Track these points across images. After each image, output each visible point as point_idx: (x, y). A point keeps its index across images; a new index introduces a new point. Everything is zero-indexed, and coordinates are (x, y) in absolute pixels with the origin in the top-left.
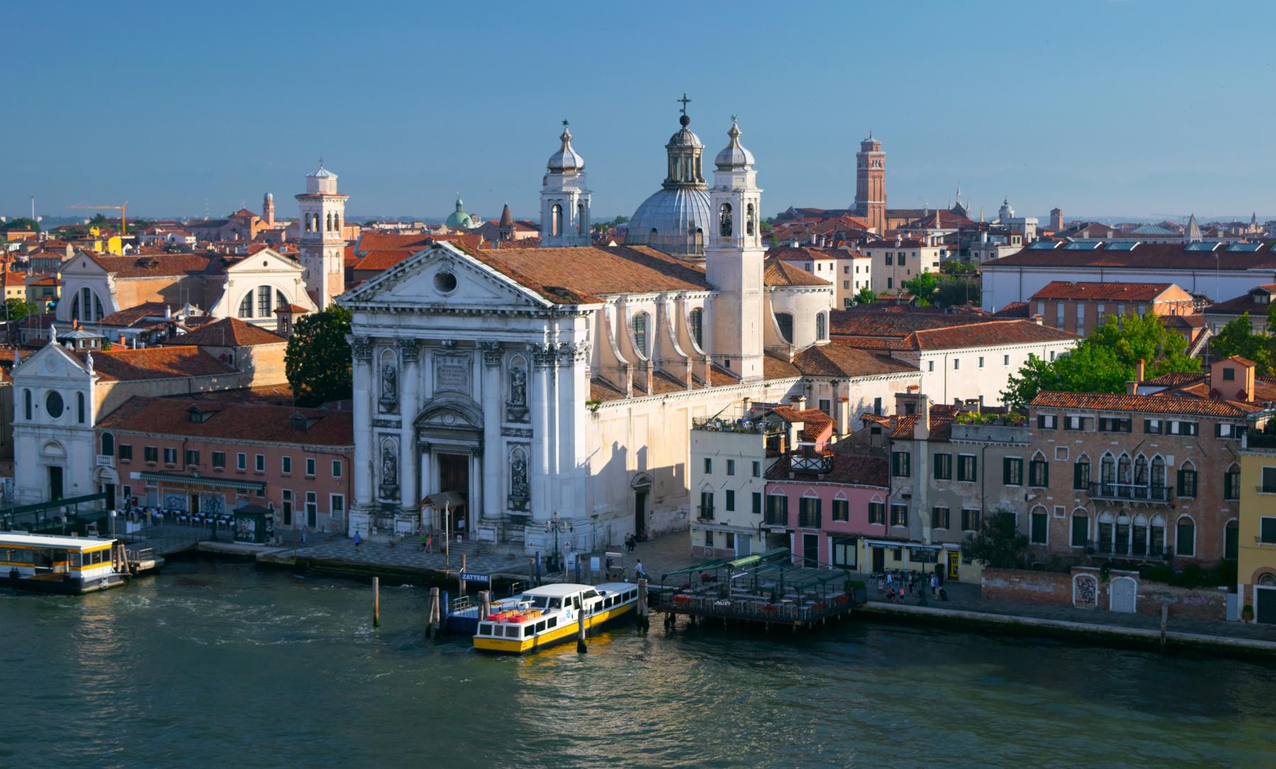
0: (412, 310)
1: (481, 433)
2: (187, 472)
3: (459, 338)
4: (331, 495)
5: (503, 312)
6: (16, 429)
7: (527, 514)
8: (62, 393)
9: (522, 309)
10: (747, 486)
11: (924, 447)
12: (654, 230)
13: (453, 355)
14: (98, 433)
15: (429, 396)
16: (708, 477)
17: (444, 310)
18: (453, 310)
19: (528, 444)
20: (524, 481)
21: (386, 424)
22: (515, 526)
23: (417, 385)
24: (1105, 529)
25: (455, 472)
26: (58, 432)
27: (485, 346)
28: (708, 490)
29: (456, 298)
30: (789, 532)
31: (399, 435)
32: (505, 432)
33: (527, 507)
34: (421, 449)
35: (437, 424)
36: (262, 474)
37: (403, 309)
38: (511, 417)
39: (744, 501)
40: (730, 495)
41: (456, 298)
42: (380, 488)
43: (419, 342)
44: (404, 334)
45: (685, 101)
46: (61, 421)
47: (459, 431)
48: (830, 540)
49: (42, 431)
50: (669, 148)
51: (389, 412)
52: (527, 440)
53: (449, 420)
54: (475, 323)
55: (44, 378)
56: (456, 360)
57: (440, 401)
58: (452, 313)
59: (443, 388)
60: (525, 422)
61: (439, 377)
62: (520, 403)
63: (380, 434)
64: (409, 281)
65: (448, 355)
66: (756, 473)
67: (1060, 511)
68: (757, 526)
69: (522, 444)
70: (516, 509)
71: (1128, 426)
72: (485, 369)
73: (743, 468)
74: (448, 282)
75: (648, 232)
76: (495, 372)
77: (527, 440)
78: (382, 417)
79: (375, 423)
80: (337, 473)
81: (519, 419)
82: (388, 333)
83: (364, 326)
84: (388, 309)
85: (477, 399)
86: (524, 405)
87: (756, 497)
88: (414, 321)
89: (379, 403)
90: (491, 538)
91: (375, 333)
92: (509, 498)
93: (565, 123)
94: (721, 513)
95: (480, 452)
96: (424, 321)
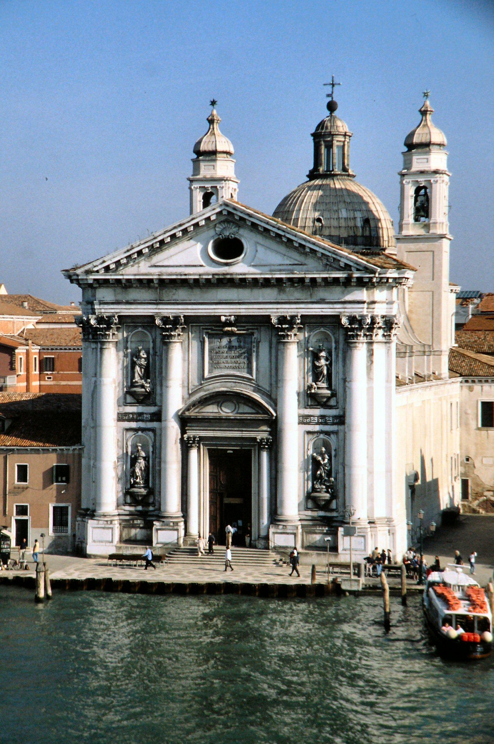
5: (313, 280)
7: (335, 514)
9: (341, 275)
18: (243, 280)
19: (336, 433)
31: (153, 430)
35: (211, 415)
42: (127, 493)
45: (333, 85)
54: (270, 294)
59: (217, 373)
60: (331, 407)
61: (211, 358)
63: (128, 430)
74: (228, 249)
77: (334, 428)
83: (113, 303)
84: (151, 281)
88: (182, 294)
93: (213, 103)
96: (197, 295)
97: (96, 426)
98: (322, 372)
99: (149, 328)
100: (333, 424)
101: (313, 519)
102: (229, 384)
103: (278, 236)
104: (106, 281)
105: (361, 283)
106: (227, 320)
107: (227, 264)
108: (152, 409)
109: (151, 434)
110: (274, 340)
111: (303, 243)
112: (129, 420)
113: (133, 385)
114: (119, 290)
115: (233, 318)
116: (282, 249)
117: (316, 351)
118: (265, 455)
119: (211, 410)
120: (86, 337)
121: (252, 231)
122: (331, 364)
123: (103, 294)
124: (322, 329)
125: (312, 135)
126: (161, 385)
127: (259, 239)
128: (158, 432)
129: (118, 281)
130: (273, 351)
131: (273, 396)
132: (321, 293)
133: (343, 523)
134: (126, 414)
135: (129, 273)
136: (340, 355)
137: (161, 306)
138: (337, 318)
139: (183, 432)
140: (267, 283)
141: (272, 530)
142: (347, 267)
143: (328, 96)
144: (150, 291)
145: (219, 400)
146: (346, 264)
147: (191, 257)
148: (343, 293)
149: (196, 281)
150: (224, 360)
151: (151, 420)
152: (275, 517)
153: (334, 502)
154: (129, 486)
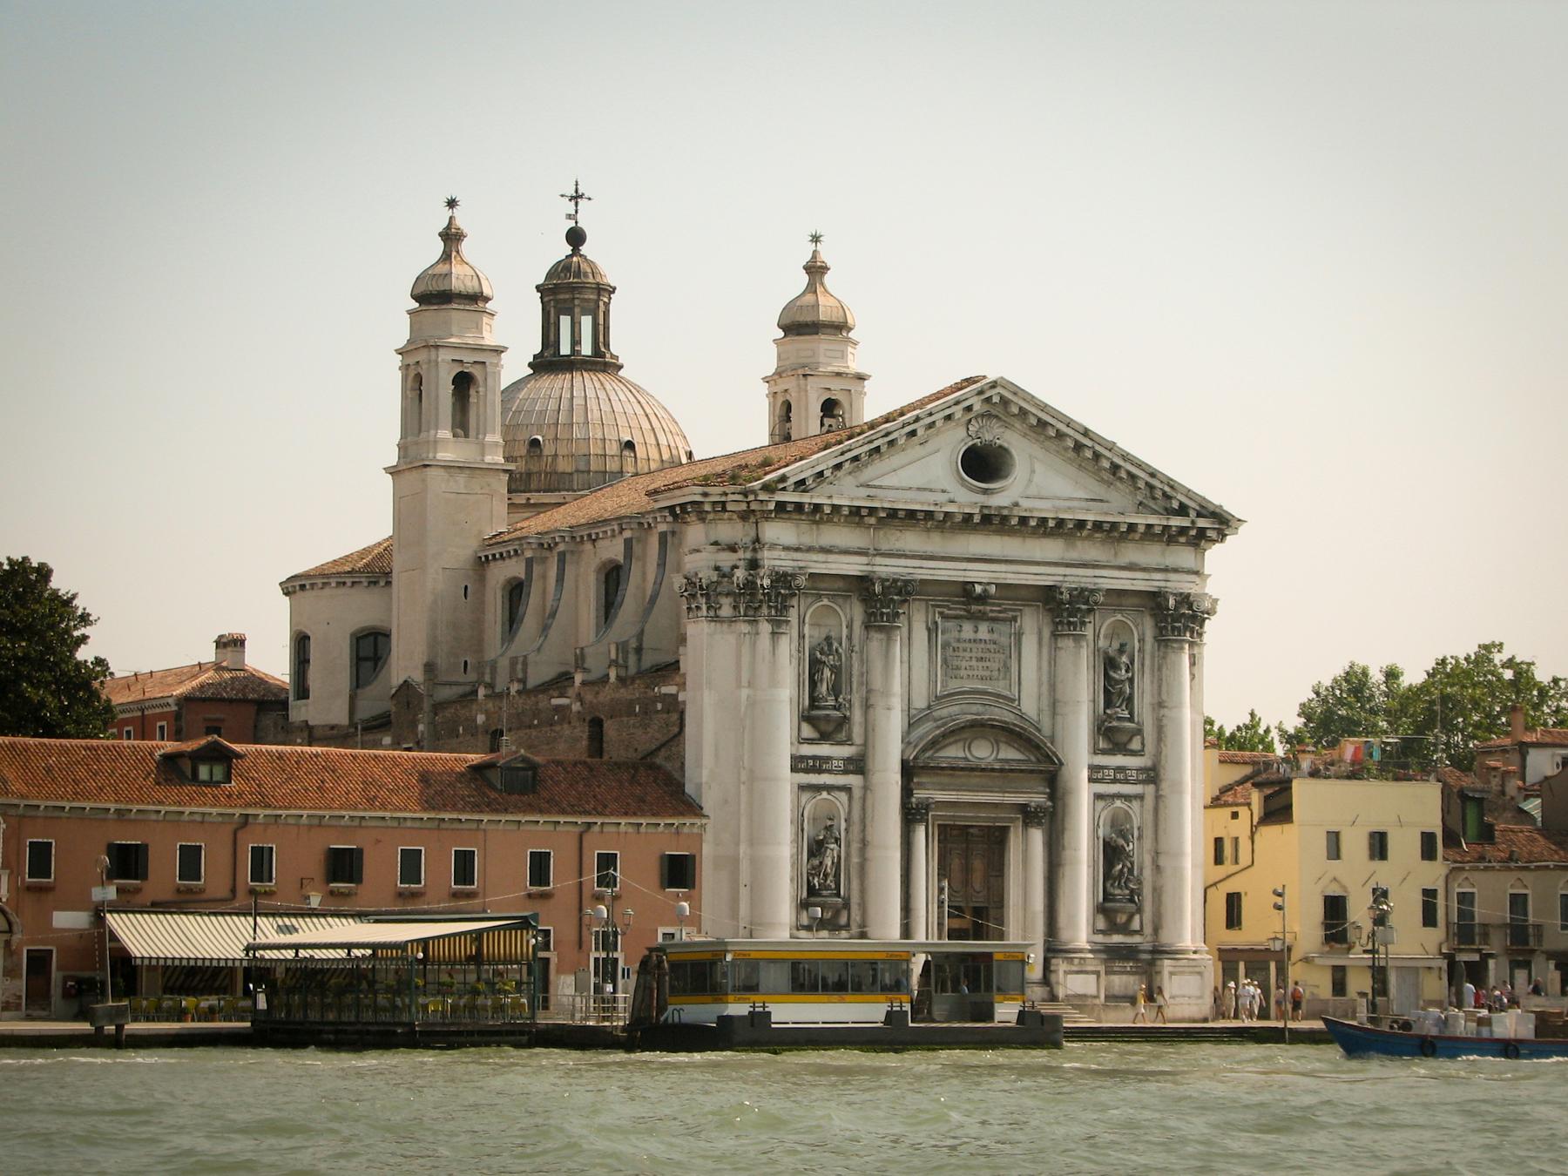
0: (929, 515)
3: (1012, 579)
4: (661, 931)
7: (1137, 939)
9: (1176, 522)
10: (1410, 875)
12: (630, 445)
13: (982, 617)
15: (920, 702)
17: (1004, 519)
18: (1023, 520)
19: (1141, 797)
20: (1131, 871)
22: (1118, 965)
23: (902, 680)
28: (1334, 891)
29: (1006, 494)
30: (1485, 957)
31: (847, 789)
32: (1096, 773)
33: (1136, 925)
34: (911, 814)
36: (471, 895)
37: (911, 514)
38: (1102, 745)
39: (1405, 908)
40: (1380, 895)
41: (1006, 494)
44: (887, 568)
45: (576, 197)
48: (1552, 965)
51: (824, 737)
52: (1137, 789)
53: (982, 752)
54: (1051, 549)
56: (984, 628)
59: (954, 685)
60: (1134, 753)
61: (945, 661)
62: (1126, 714)
63: (803, 788)
66: (1428, 852)
68: (1432, 948)
69: (1127, 798)
72: (1070, 643)
73: (1404, 845)
74: (983, 464)
75: (613, 449)
77: (1137, 789)
78: (807, 750)
79: (798, 764)
81: (1119, 748)
82: (852, 566)
83: (797, 549)
85: (1029, 706)
86: (1131, 719)
88: (911, 540)
89: (806, 718)
90: (1092, 990)
93: (452, 203)
95: (1051, 819)
97: (754, 779)
98: (1121, 692)
99: (840, 601)
100: (1137, 782)
102: (974, 709)
103: (1078, 447)
104: (799, 507)
106: (985, 591)
107: (985, 492)
108: (846, 751)
109: (843, 796)
110: (1046, 633)
111: (1121, 463)
112: (807, 771)
113: (814, 700)
114: (804, 526)
115: (993, 589)
116: (1072, 470)
117: (1111, 652)
118: (1037, 837)
119: (953, 752)
120: (712, 613)
121: (1025, 436)
122: (1131, 680)
123: (777, 532)
124: (1119, 617)
125: (538, 288)
126: (867, 706)
127: (1036, 450)
128: (857, 793)
129: (817, 508)
130: (1045, 650)
131: (1046, 730)
133: (1158, 952)
134: (803, 758)
136: (1147, 662)
137: (879, 560)
139: (907, 792)
141: (1060, 966)
142: (1183, 510)
143: (569, 217)
144: (858, 531)
145: (964, 736)
146: (1181, 504)
147: (930, 475)
148: (1163, 554)
150: (964, 664)
151: (846, 772)
153: (1137, 917)
154: (805, 895)
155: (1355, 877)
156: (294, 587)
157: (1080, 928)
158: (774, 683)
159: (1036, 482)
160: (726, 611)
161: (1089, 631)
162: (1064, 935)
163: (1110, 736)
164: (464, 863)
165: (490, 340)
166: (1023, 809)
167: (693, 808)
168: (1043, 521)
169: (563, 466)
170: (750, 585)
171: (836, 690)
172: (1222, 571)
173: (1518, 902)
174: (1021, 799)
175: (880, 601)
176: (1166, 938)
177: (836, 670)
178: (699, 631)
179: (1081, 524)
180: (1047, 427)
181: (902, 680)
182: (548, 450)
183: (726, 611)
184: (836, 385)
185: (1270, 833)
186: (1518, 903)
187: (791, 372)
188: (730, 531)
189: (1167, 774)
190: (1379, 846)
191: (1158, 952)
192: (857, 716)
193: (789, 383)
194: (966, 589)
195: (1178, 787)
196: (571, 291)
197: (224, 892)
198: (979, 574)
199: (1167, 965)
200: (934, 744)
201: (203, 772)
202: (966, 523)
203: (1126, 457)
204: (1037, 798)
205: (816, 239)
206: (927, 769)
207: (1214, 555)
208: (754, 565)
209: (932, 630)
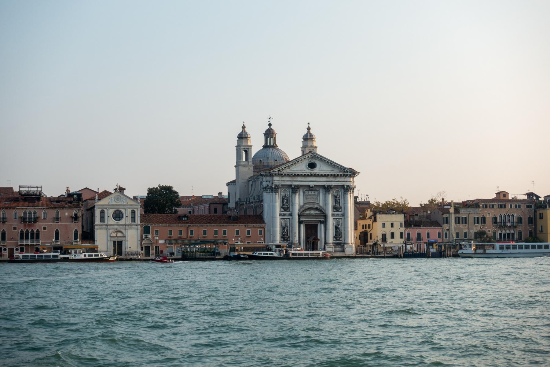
0: (301, 175)
1: (325, 216)
2: (188, 238)
6: (96, 227)
8: (123, 211)
9: (346, 174)
10: (398, 230)
11: (453, 215)
13: (313, 190)
14: (142, 226)
15: (302, 204)
16: (384, 229)
18: (318, 175)
21: (284, 215)
23: (298, 201)
24: (500, 234)
25: (312, 231)
26: (120, 226)
27: (329, 186)
28: (384, 233)
29: (316, 171)
32: (333, 215)
34: (300, 222)
37: (298, 175)
39: (397, 235)
41: (316, 171)
43: (302, 186)
46: (122, 222)
47: (316, 216)
49: (111, 227)
50: (265, 134)
51: (285, 211)
53: (312, 212)
55: (113, 205)
56: (313, 192)
57: (307, 206)
58: (318, 175)
59: (308, 201)
64: (297, 165)
65: (310, 190)
66: (401, 226)
67: (489, 231)
68: (402, 242)
70: (337, 240)
71: (505, 206)
74: (312, 166)
76: (330, 195)
78: (282, 213)
79: (280, 215)
80: (260, 233)
81: (337, 211)
85: (321, 204)
87: (401, 234)
88: (299, 179)
89: (282, 207)
91: (283, 183)
92: (334, 237)
94: (389, 240)
95: (325, 222)
97: (273, 218)
101: (336, 243)
105: (350, 176)
113: (283, 205)
118: (323, 226)
119: (307, 212)
123: (276, 178)
126: (292, 205)
127: (321, 163)
132: (338, 179)
133: (344, 244)
135: (285, 172)
138: (343, 186)
139: (299, 219)
140: (325, 176)
141: (326, 246)
147: (302, 168)
149: (305, 175)
152: (326, 243)
155: (388, 230)
156: (228, 184)
157: (331, 240)
158: (276, 202)
159: (321, 168)
160: (268, 191)
161: (332, 192)
162: (327, 241)
163: (335, 208)
164: (225, 232)
165: (249, 144)
166: (320, 221)
167: (264, 222)
168: (322, 175)
169: (265, 164)
170: (271, 187)
171: (287, 203)
172: (356, 181)
173: (419, 234)
174: (319, 219)
175: (294, 189)
176: (346, 242)
177: (287, 200)
178: (265, 194)
179: (328, 175)
180: (322, 159)
181: (298, 201)
182: (263, 161)
183: (268, 191)
184: (311, 149)
185: (374, 223)
186: (419, 234)
187: (304, 147)
188: (269, 178)
189: (345, 215)
190: (392, 225)
191: (344, 244)
192: (291, 207)
193: (303, 149)
194: (309, 186)
195: (347, 217)
196: (269, 134)
197: (185, 237)
198: (311, 184)
199: (345, 246)
200: (304, 211)
201: (184, 219)
202: (308, 176)
203: (336, 163)
204: (322, 219)
205: (309, 124)
206: (304, 215)
207: (355, 178)
208: (273, 184)
209: (304, 193)
